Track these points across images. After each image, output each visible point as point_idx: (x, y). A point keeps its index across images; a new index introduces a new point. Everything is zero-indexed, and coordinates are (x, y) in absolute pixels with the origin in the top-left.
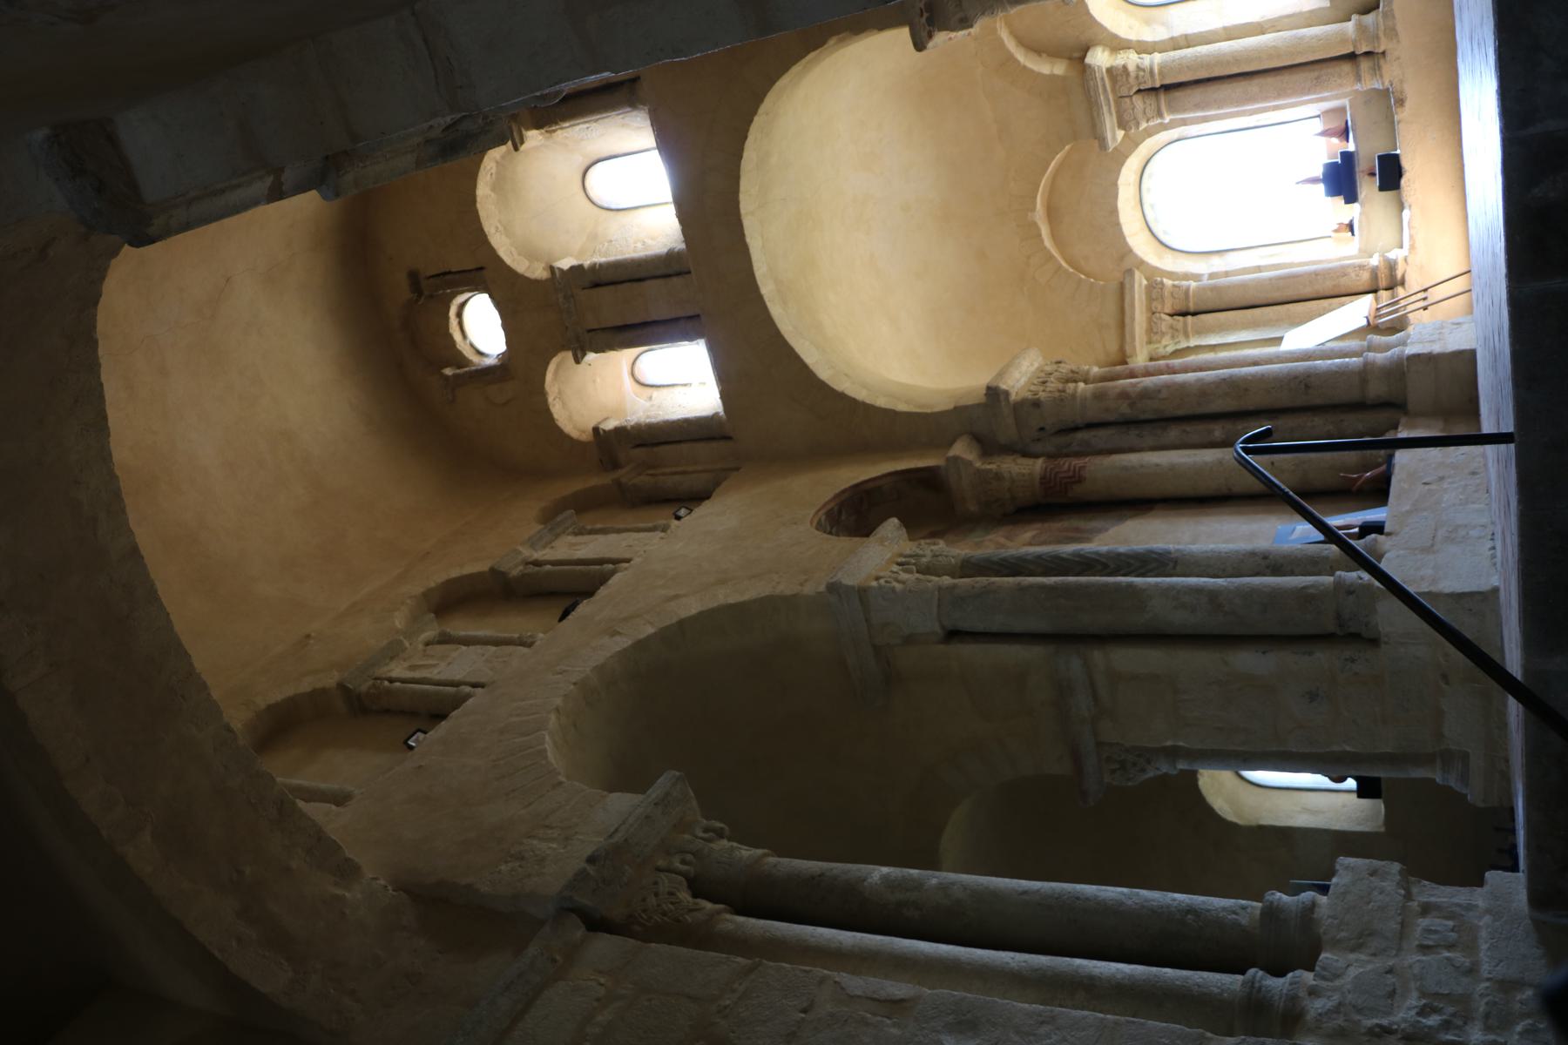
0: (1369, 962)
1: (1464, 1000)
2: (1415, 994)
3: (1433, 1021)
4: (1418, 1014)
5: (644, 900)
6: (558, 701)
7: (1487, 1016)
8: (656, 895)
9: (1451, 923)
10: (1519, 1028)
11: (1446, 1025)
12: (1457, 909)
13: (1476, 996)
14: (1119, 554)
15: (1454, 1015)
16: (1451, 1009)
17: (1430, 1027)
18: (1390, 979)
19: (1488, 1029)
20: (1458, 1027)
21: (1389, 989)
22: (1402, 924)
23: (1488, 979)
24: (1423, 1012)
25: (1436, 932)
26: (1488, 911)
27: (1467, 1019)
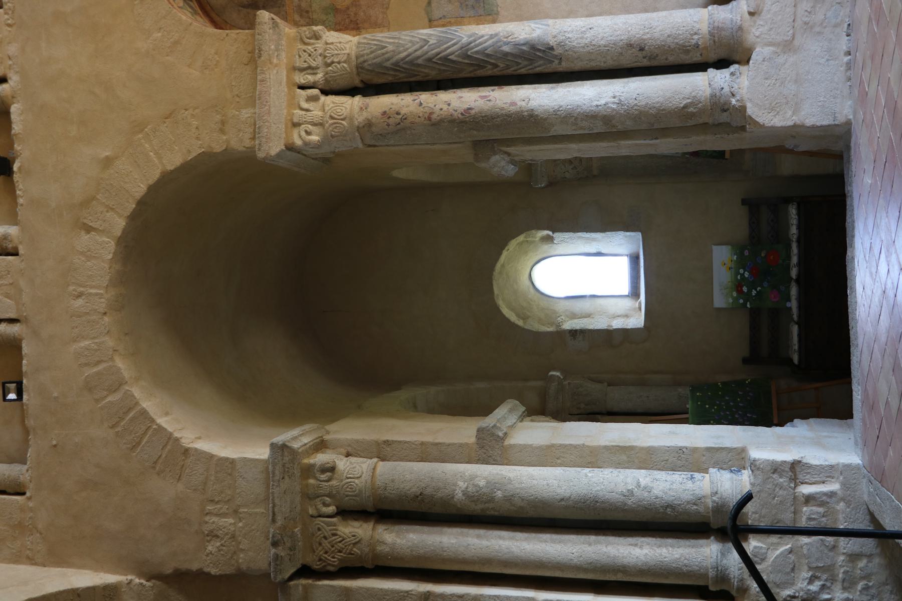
0: (778, 544)
1: (829, 569)
2: (806, 567)
3: (815, 587)
4: (809, 584)
5: (320, 544)
6: (110, 342)
7: (844, 580)
8: (325, 538)
9: (821, 510)
10: (859, 587)
11: (823, 587)
12: (824, 498)
13: (837, 566)
14: (506, 54)
15: (826, 580)
16: (825, 577)
17: (815, 593)
18: (792, 557)
19: (844, 589)
20: (829, 588)
21: (791, 566)
22: (795, 513)
23: (844, 554)
24: (811, 581)
25: (814, 519)
26: (843, 499)
27: (833, 579)
